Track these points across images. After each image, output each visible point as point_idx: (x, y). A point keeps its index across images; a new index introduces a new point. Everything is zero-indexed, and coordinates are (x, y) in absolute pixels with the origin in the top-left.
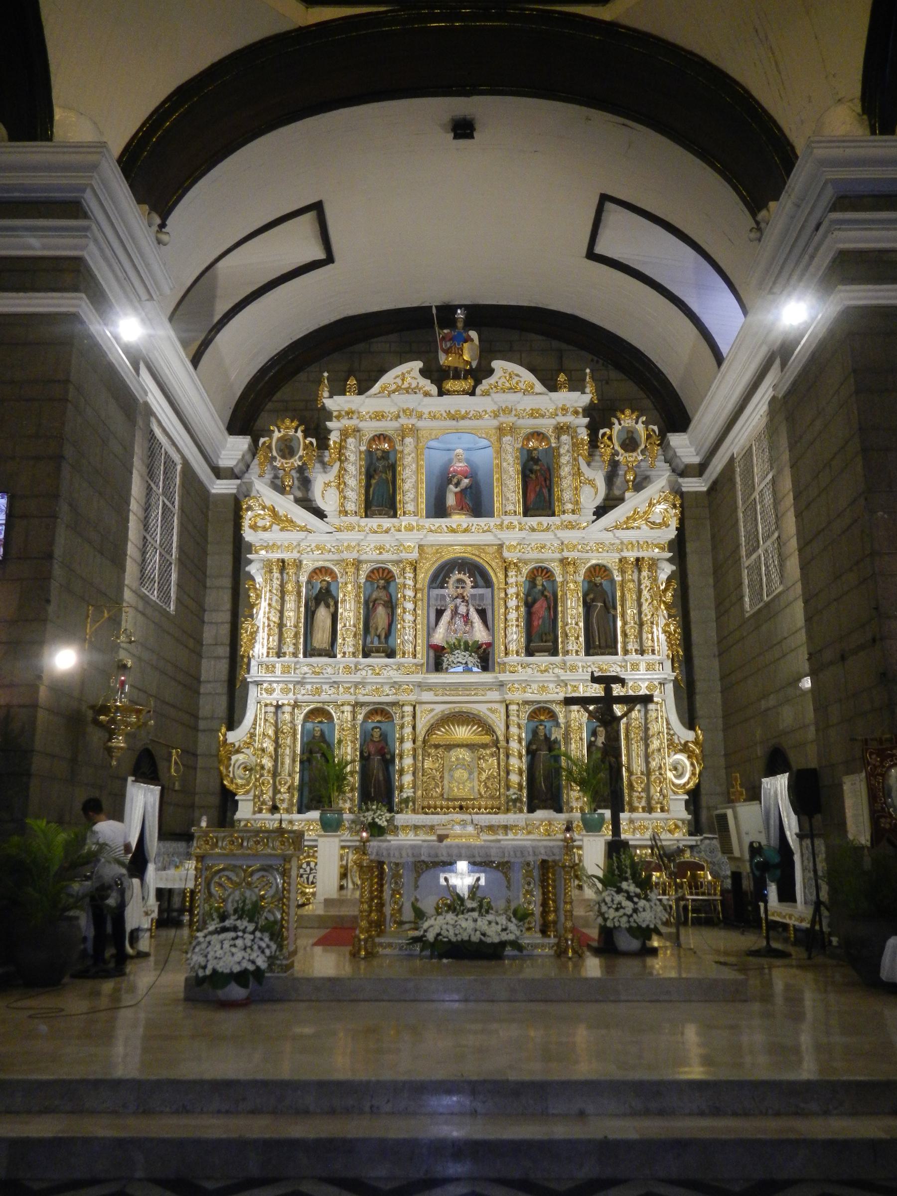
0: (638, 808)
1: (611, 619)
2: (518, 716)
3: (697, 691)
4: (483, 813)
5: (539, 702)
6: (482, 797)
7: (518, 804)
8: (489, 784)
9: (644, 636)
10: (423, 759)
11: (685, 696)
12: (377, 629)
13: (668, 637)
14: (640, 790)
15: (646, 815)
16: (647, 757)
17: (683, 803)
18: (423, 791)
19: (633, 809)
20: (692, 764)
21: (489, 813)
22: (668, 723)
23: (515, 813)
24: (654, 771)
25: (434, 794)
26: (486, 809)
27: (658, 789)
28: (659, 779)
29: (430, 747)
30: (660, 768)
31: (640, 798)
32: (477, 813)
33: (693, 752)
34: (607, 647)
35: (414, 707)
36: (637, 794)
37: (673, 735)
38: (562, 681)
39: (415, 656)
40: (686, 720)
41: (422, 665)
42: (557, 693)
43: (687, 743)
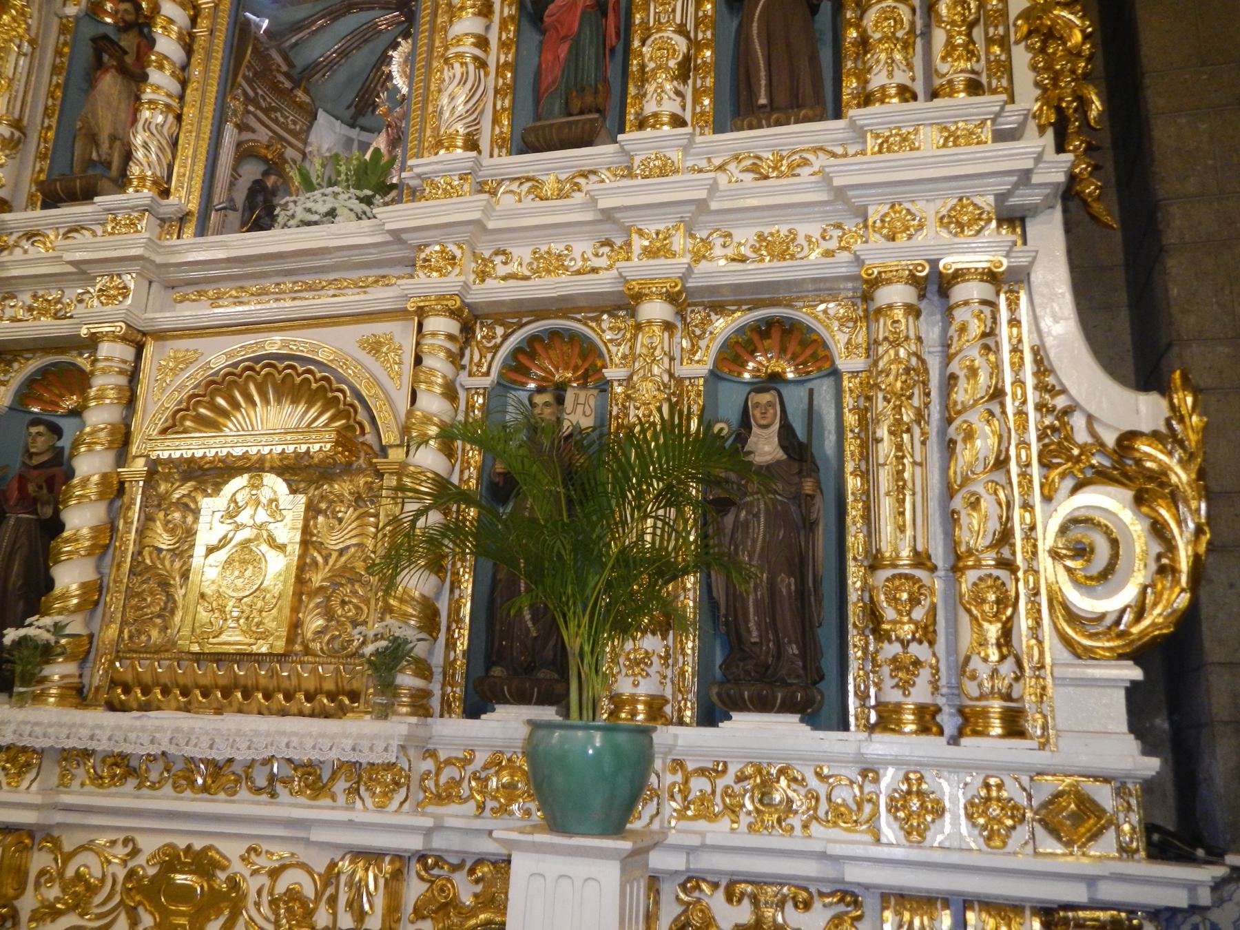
0: (898, 708)
1: (829, 36)
2: (455, 359)
3: (1170, 238)
4: (301, 714)
5: (539, 309)
6: (307, 651)
7: (407, 680)
8: (335, 603)
9: (939, 36)
10: (148, 519)
11: (1122, 297)
12: (93, 139)
13: (1043, 50)
14: (907, 630)
15: (935, 746)
16: (949, 492)
17: (1119, 699)
18: (124, 623)
19: (887, 720)
20: (1158, 530)
21: (327, 715)
22: (1043, 366)
23: (384, 713)
24: (970, 552)
25: (155, 634)
26: (309, 698)
27: (993, 631)
28: (1000, 587)
29: (167, 477)
30: (1005, 537)
31: (906, 668)
32: (283, 713)
33: (1160, 477)
34: (800, 107)
35: (140, 348)
36: (896, 648)
37: (1067, 411)
38: (608, 215)
39: (165, 193)
40: (1129, 368)
41: (183, 219)
42: (594, 270)
43: (1128, 439)
